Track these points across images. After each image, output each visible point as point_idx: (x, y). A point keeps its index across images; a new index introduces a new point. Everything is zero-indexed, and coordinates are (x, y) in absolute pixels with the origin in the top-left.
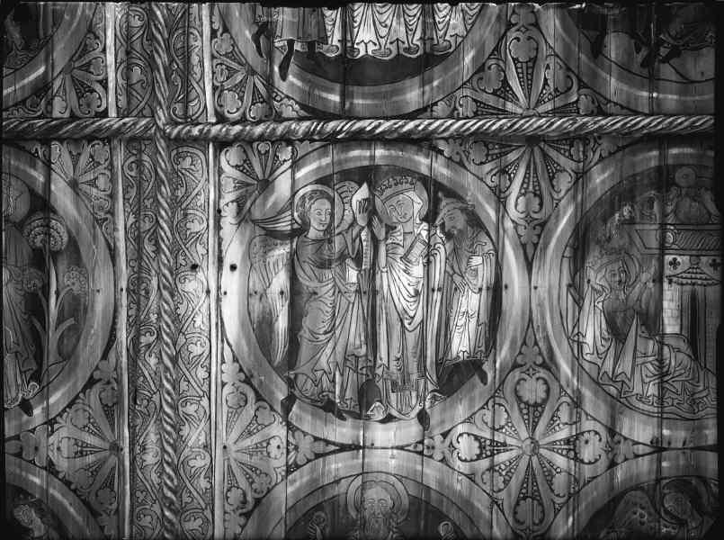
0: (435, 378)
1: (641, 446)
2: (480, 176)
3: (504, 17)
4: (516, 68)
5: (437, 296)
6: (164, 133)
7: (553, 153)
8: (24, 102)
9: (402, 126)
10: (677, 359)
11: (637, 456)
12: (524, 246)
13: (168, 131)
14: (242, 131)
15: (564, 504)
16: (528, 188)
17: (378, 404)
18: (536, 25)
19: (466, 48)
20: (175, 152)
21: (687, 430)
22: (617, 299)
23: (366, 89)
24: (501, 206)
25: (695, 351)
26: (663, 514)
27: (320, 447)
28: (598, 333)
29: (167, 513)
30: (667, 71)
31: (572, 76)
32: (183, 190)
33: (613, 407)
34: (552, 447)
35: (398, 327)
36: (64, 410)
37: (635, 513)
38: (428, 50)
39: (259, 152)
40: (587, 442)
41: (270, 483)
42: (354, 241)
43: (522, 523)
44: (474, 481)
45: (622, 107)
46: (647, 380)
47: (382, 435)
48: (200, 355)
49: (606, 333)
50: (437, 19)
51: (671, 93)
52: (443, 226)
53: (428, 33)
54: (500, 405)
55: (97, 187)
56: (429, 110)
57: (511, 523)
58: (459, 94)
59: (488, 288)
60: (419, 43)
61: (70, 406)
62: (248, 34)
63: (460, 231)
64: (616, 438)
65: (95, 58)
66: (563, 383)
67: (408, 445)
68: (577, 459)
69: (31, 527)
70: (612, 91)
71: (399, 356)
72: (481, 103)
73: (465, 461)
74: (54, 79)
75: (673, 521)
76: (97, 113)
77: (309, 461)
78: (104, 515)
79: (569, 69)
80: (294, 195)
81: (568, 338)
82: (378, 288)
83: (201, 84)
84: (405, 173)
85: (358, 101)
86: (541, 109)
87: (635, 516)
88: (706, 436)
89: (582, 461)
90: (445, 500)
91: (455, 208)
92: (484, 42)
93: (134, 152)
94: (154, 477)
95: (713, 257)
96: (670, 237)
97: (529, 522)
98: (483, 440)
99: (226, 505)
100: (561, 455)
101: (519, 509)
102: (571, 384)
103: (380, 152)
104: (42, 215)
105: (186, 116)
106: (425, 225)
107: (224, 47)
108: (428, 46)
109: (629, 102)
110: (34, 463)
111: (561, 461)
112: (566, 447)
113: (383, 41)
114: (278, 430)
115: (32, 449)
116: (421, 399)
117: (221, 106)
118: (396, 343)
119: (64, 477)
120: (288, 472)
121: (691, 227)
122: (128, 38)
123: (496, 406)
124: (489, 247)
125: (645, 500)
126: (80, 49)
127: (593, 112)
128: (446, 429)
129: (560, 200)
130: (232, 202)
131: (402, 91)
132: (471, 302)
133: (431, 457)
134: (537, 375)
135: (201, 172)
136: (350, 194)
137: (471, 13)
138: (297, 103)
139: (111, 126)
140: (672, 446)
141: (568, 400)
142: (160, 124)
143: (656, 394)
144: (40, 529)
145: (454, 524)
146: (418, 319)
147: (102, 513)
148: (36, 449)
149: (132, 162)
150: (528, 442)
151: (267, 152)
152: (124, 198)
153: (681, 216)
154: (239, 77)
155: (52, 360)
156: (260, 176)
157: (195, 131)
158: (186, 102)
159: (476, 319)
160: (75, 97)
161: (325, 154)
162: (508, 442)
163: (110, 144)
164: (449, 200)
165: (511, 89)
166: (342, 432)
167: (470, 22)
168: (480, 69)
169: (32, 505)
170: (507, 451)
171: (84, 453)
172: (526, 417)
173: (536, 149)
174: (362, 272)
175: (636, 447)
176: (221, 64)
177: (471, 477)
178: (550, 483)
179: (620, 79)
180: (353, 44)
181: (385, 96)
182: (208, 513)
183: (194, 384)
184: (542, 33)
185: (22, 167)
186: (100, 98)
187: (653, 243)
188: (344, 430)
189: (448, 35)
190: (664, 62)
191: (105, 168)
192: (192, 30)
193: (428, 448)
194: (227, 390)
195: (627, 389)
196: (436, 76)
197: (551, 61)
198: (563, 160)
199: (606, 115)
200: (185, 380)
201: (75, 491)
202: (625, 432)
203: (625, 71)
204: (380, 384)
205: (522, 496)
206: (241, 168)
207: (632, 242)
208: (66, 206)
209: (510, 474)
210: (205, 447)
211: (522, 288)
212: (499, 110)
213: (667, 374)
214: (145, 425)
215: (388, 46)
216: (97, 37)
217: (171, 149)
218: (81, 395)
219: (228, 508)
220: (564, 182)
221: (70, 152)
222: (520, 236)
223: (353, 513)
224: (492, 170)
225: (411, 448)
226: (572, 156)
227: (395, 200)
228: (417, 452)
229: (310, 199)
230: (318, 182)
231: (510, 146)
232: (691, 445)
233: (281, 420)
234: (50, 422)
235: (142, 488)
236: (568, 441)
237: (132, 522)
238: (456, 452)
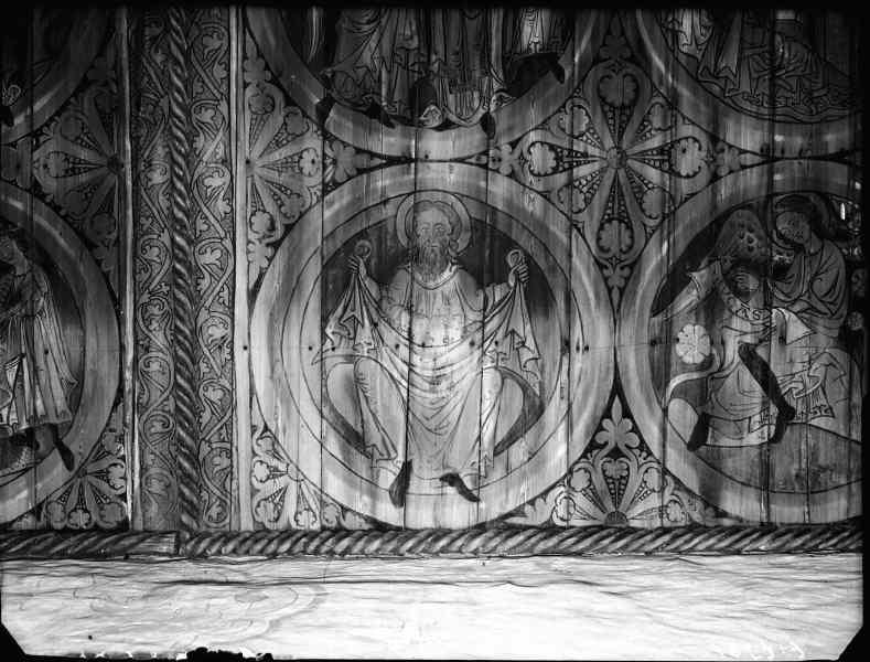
0: (501, 75)
11: (744, 167)
15: (657, 227)
17: (433, 107)
21: (803, 136)
26: (776, 239)
27: (363, 161)
29: (178, 239)
33: (715, 109)
36: (51, 119)
37: (742, 238)
40: (684, 151)
41: (303, 206)
43: (608, 250)
44: (549, 200)
47: (437, 145)
48: (216, 50)
54: (580, 107)
61: (58, 113)
64: (720, 145)
66: (655, 80)
67: (470, 157)
68: (674, 173)
69: (11, 262)
71: (458, 49)
73: (539, 175)
75: (789, 246)
77: (350, 178)
78: (102, 246)
88: (827, 143)
89: (679, 175)
90: (515, 223)
94: (163, 202)
97: (614, 249)
99: (250, 232)
100: (654, 167)
101: (604, 235)
102: (664, 82)
110: (16, 185)
111: (653, 175)
114: (313, 142)
115: (12, 166)
116: (485, 100)
119: (52, 201)
120: (325, 192)
123: (576, 108)
128: (517, 136)
133: (497, 171)
140: (787, 155)
141: (661, 100)
143: (767, 92)
144: (22, 265)
145: (525, 252)
147: (99, 244)
148: (18, 166)
150: (614, 152)
155: (37, 58)
162: (590, 152)
166: (388, 142)
169: (13, 236)
170: (589, 162)
171: (77, 171)
172: (611, 122)
175: (743, 156)
177: (545, 195)
182: (227, 243)
183: (210, 85)
188: (392, 140)
193: (494, 160)
194: (249, 92)
200: (198, 81)
201: (64, 218)
202: (730, 139)
210: (224, 162)
214: (150, 138)
218: (72, 100)
219: (252, 237)
223: (403, 241)
225: (473, 160)
228: (477, 165)
233: (315, 128)
234: (35, 135)
235: (148, 213)
236: (661, 150)
237: (135, 256)
238: (526, 166)
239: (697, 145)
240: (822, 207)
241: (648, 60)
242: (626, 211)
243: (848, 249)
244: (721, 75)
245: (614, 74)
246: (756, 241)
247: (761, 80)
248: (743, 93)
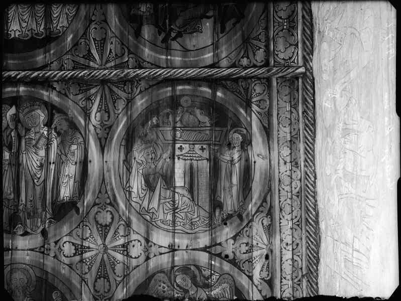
1: (163, 248)
2: (76, 101)
4: (95, 44)
5: (52, 167)
7: (115, 89)
9: (31, 74)
10: (182, 199)
11: (161, 254)
12: (100, 139)
15: (121, 281)
17: (20, 225)
18: (105, 21)
21: (188, 239)
22: (150, 168)
25: (193, 197)
26: (176, 287)
28: (140, 187)
30: (175, 45)
31: (125, 47)
33: (148, 227)
34: (115, 249)
35: (31, 184)
38: (48, 34)
40: (134, 246)
42: (8, 137)
45: (152, 64)
46: (166, 212)
47: (22, 243)
49: (144, 186)
50: (53, 18)
51: (178, 57)
52: (55, 128)
53: (48, 24)
54: (86, 226)
57: (92, 291)
59: (80, 162)
63: (65, 131)
64: (150, 244)
66: (121, 213)
67: (36, 248)
70: (146, 55)
71: (32, 199)
72: (76, 62)
73: (67, 257)
79: (123, 44)
81: (124, 189)
82: (21, 162)
86: (108, 65)
87: (159, 288)
89: (131, 257)
90: (56, 279)
91: (62, 119)
92: (78, 30)
95: (201, 145)
96: (178, 134)
97: (102, 292)
98: (77, 245)
100: (120, 253)
101: (97, 284)
102: (125, 214)
103: (22, 89)
106: (46, 128)
108: (48, 32)
109: (155, 62)
112: (122, 249)
113: (24, 30)
116: (43, 222)
118: (30, 193)
121: (190, 129)
124: (81, 140)
125: (166, 279)
127: (136, 67)
128: (58, 239)
129: (119, 114)
131: (34, 56)
132: (71, 169)
133: (48, 255)
134: (107, 209)
136: (6, 112)
137: (71, 15)
140: (180, 248)
141: (123, 223)
143: (171, 220)
145: (61, 293)
146: (42, 179)
153: (184, 123)
159: (73, 179)
164: (59, 115)
165: (92, 55)
167: (70, 19)
168: (76, 44)
170: (90, 251)
172: (101, 232)
173: (106, 86)
174: (12, 154)
175: (161, 248)
177: (70, 266)
178: (114, 270)
179: (151, 49)
187: (169, 137)
189: (59, 26)
190: (173, 40)
193: (47, 250)
195: (155, 217)
196: (52, 48)
197: (113, 40)
199: (141, 67)
202: (154, 241)
203: (153, 45)
204: (21, 214)
205: (98, 276)
207: (157, 136)
209: (92, 264)
211: (98, 161)
212: (86, 66)
213: (177, 208)
215: (26, 32)
220: (121, 105)
222: (97, 134)
224: (82, 98)
225: (37, 250)
226: (125, 90)
228: (40, 252)
232: (191, 248)
236: (123, 246)
238: (62, 252)
239: (139, 243)
240: (197, 272)
241: (118, 204)
242: (107, 273)
243: (209, 292)
244: (151, 211)
245: (102, 210)
246: (166, 287)
247: (169, 213)
248: (161, 220)
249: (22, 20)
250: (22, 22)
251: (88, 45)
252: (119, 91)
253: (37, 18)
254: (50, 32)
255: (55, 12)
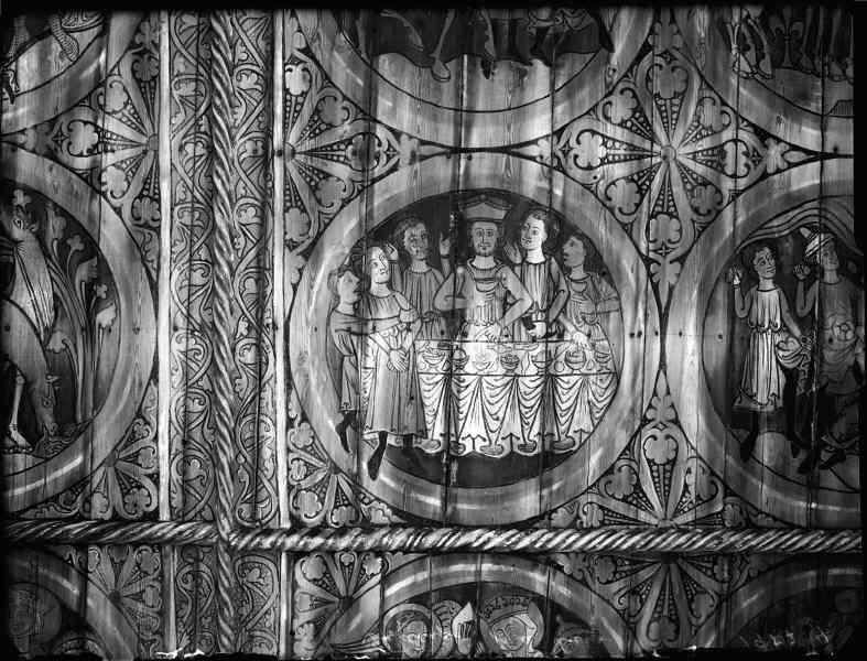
2: (606, 598)
3: (638, 411)
4: (652, 471)
6: (229, 546)
7: (692, 572)
8: (55, 498)
13: (233, 543)
14: (323, 544)
16: (662, 612)
18: (676, 422)
19: (592, 448)
20: (240, 562)
23: (472, 491)
24: (631, 633)
30: (830, 479)
31: (716, 480)
32: (249, 607)
38: (547, 448)
39: (342, 564)
45: (775, 519)
50: (559, 412)
51: (833, 505)
55: (144, 602)
56: (547, 517)
58: (583, 500)
60: (536, 439)
62: (332, 425)
65: (145, 448)
72: (609, 510)
74: (93, 472)
76: (145, 513)
79: (713, 473)
80: (383, 615)
83: (273, 481)
84: (517, 594)
85: (463, 506)
86: (681, 520)
93: (191, 560)
103: (487, 567)
104: (75, 635)
105: (253, 518)
107: (302, 439)
117: (297, 508)
122: (186, 425)
126: (125, 440)
129: (700, 627)
130: (308, 622)
131: (513, 496)
135: (270, 587)
137: (600, 405)
138: (389, 506)
139: (164, 535)
142: (224, 535)
149: (189, 573)
151: (352, 564)
152: (177, 617)
154: (320, 476)
156: (343, 593)
157: (267, 543)
158: (254, 503)
160: (120, 495)
161: (422, 568)
163: (161, 551)
167: (598, 415)
173: (673, 566)
176: (298, 459)
179: (775, 486)
180: (458, 439)
181: (493, 501)
184: (680, 427)
185: (52, 576)
186: (149, 495)
189: (571, 430)
191: (154, 580)
192: (265, 419)
196: (556, 478)
198: (704, 581)
203: (779, 475)
206: (320, 583)
208: (105, 624)
212: (631, 519)
216: (147, 423)
217: (235, 558)
221: (112, 560)
224: (619, 591)
226: (714, 574)
227: (503, 624)
229: (402, 622)
230: (412, 600)
231: (643, 562)
249: (491, 415)
250: (489, 419)
251: (635, 473)
252: (702, 576)
253: (524, 410)
254: (552, 443)
255: (564, 398)
